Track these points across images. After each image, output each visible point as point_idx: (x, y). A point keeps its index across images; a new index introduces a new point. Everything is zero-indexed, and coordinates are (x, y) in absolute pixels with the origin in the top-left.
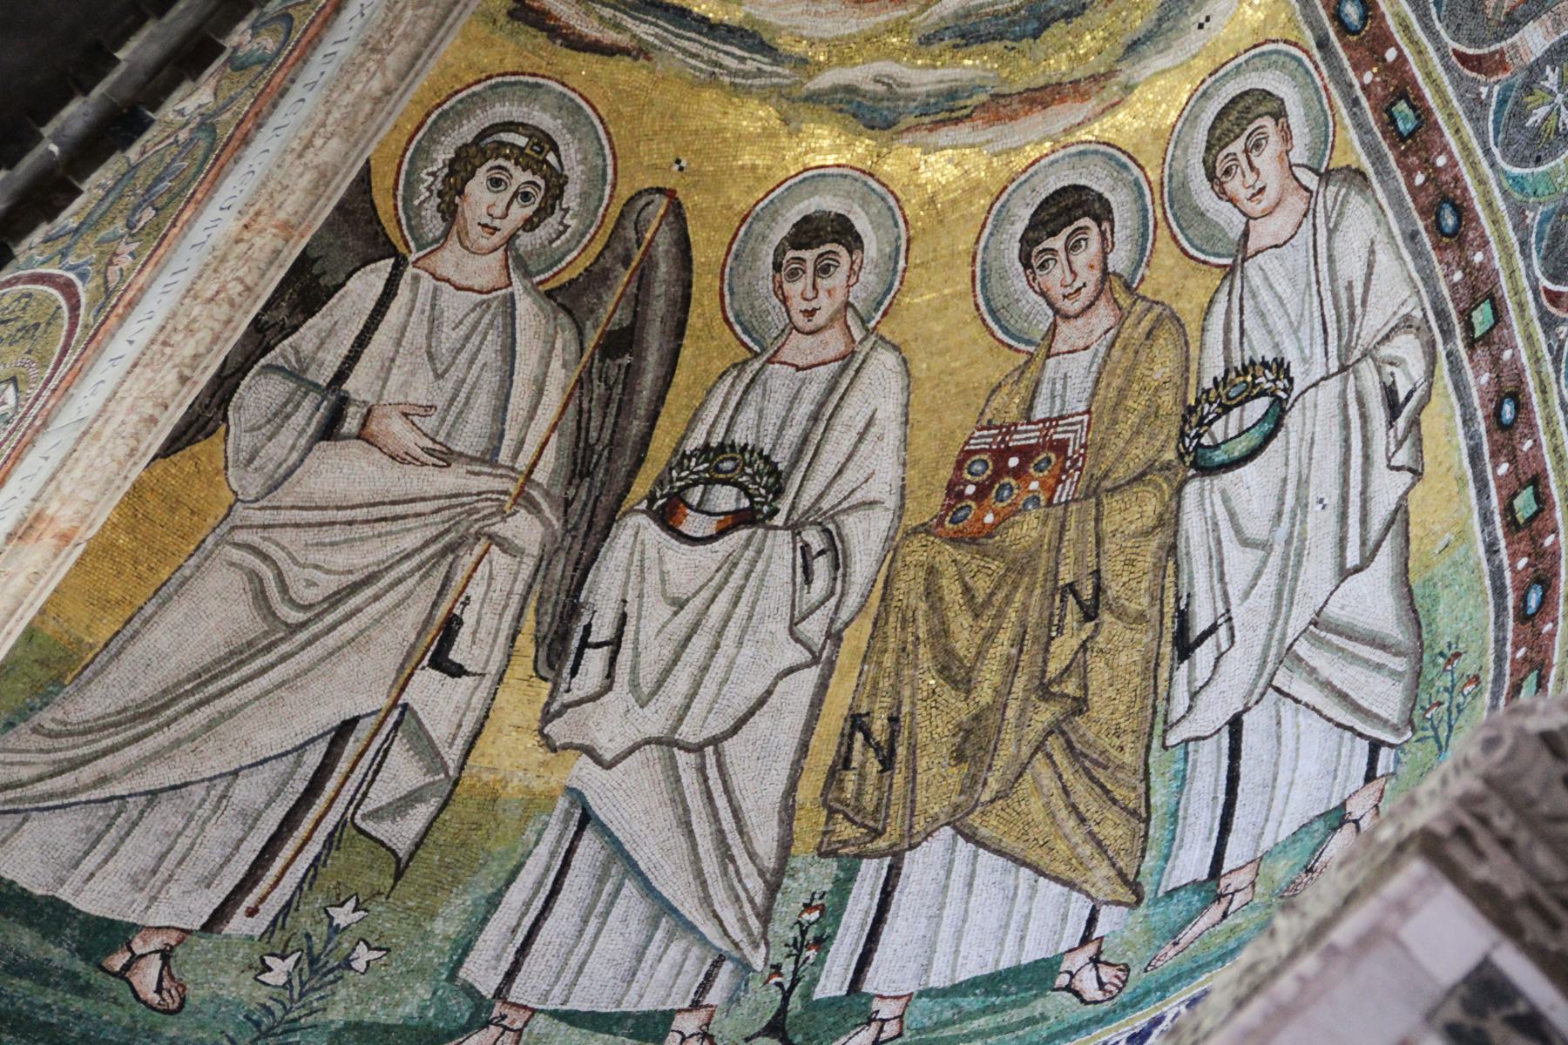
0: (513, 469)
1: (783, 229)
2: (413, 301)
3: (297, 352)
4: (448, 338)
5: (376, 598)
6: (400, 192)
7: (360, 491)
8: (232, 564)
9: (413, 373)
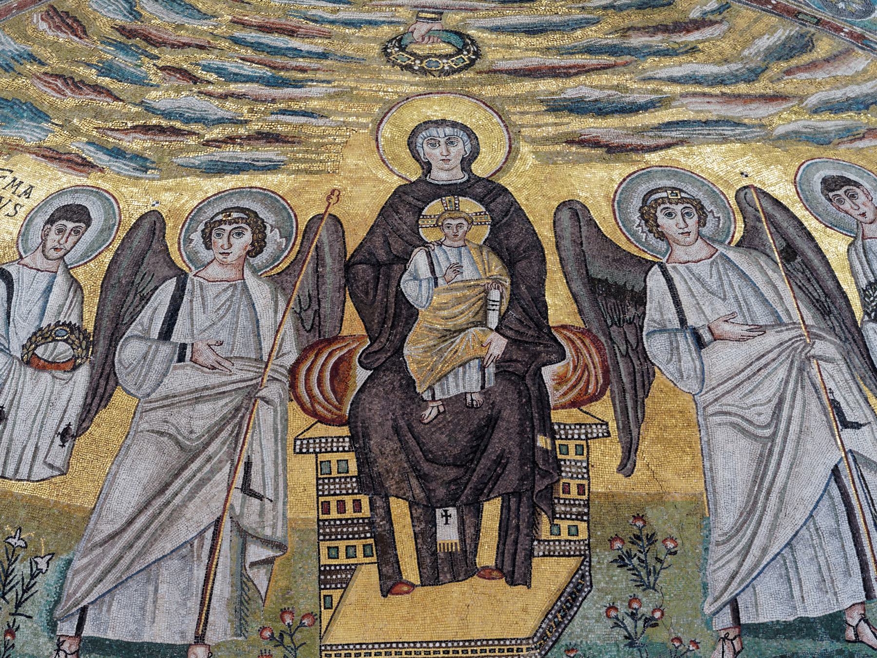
0: (794, 323)
1: (818, 187)
2: (682, 276)
3: (655, 321)
4: (713, 283)
5: (792, 407)
6: (632, 240)
8: (720, 424)
9: (711, 304)
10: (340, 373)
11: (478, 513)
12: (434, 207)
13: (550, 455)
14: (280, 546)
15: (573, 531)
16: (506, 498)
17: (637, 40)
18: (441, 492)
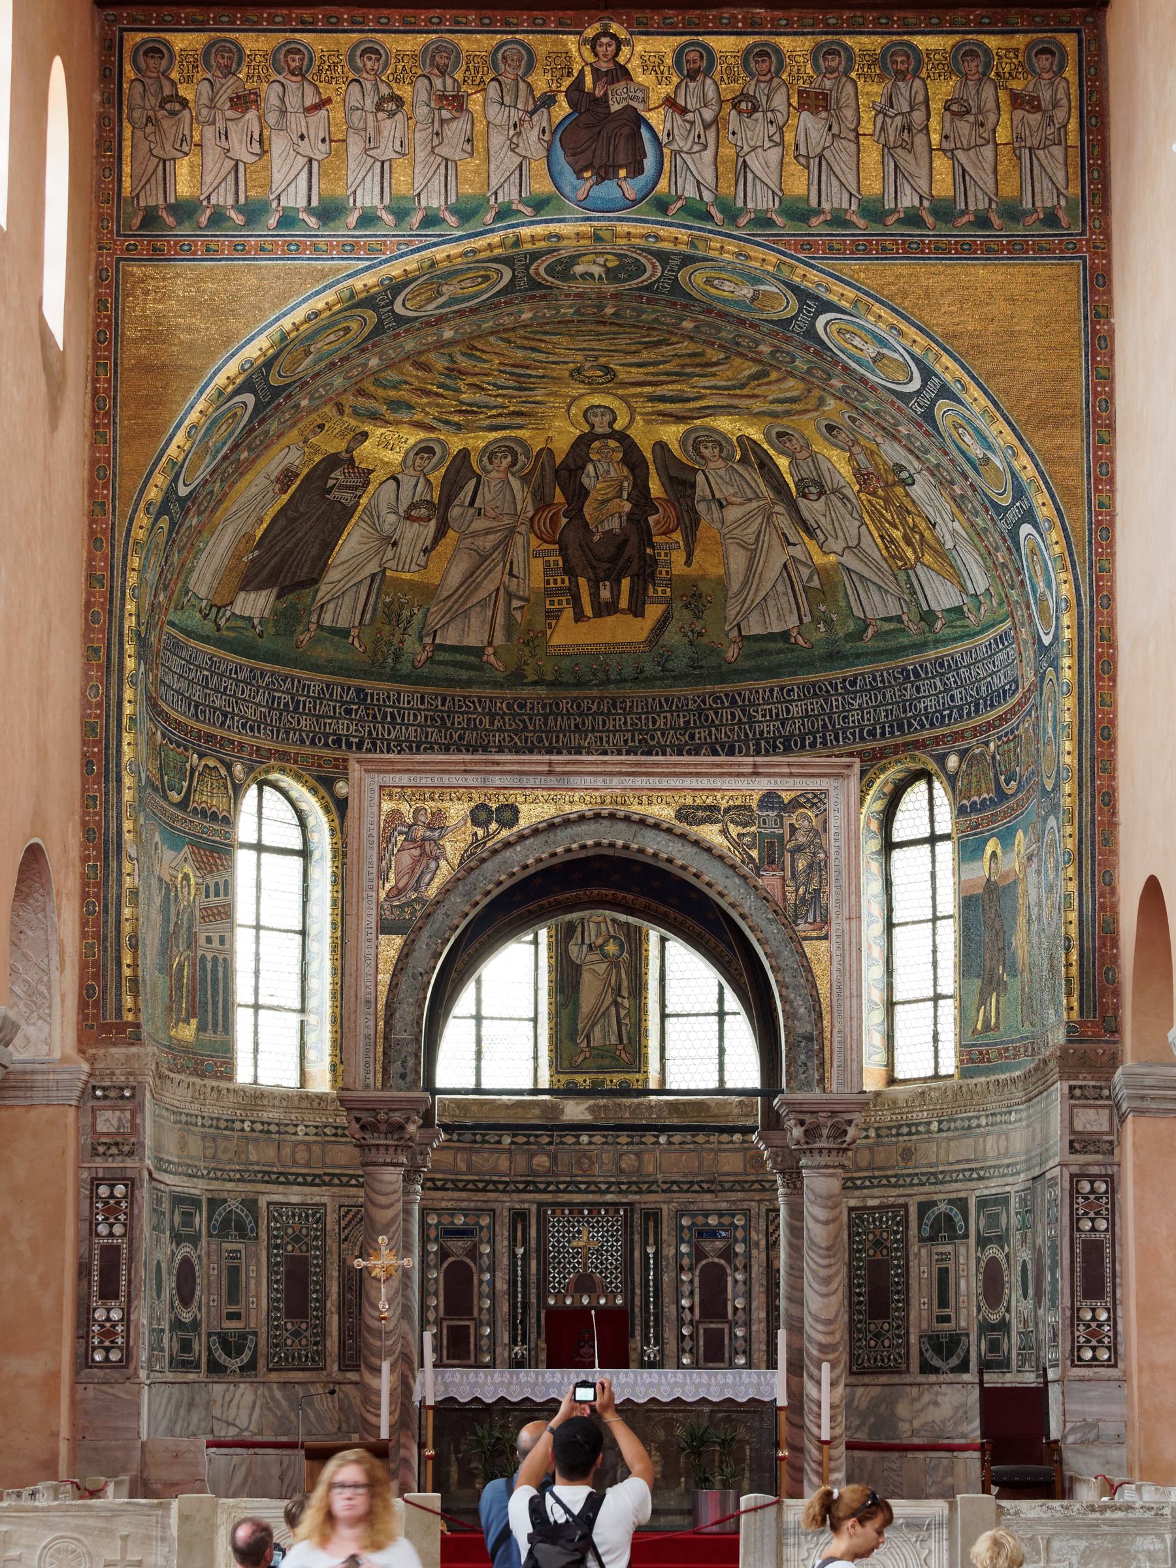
4: (727, 478)
7: (740, 515)
10: (554, 520)
11: (620, 583)
12: (597, 444)
13: (652, 557)
14: (527, 600)
15: (664, 592)
16: (632, 577)
17: (688, 370)
18: (602, 575)
